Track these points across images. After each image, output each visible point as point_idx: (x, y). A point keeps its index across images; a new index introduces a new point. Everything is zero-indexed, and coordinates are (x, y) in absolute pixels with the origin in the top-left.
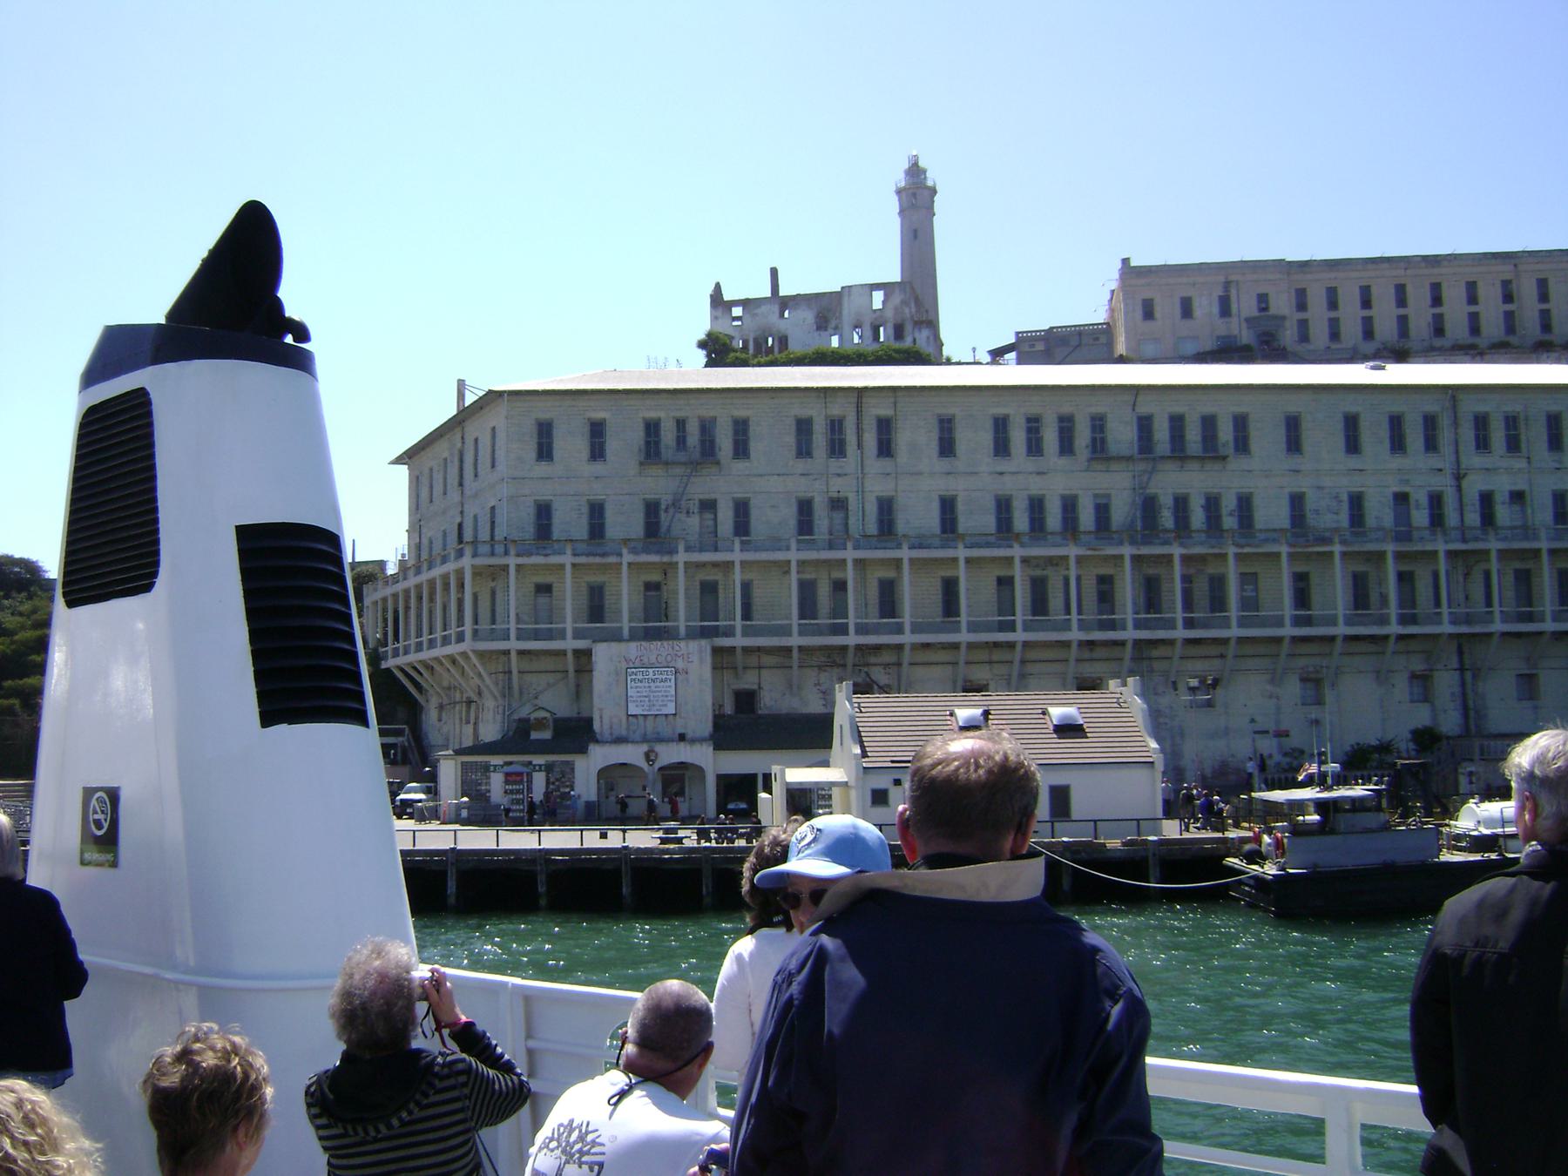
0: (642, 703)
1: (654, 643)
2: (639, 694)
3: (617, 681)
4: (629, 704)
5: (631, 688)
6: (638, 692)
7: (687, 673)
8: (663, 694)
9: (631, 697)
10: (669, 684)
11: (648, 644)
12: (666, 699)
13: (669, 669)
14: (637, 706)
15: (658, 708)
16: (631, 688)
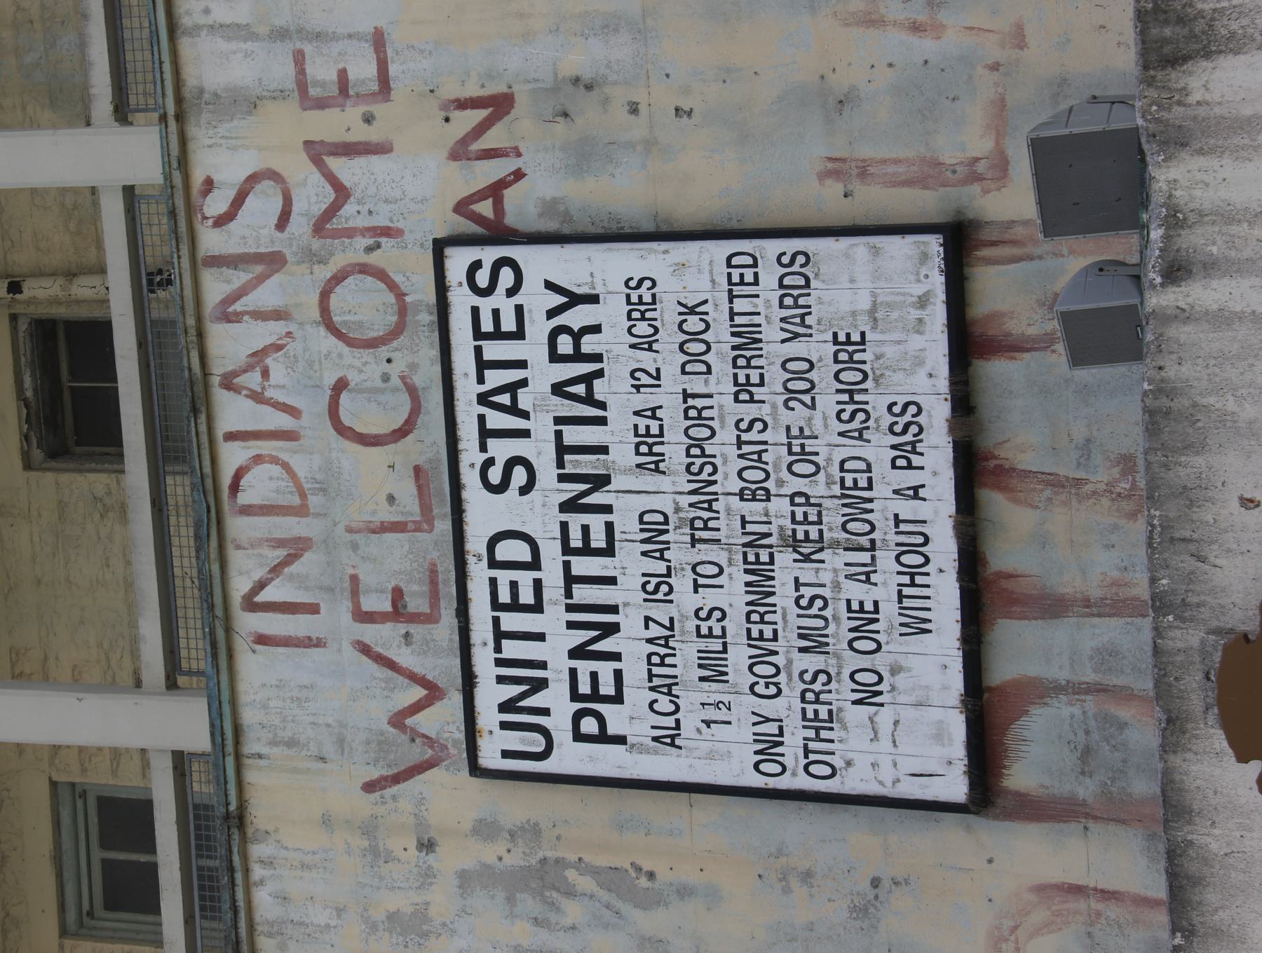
0: (839, 633)
1: (232, 456)
2: (739, 656)
3: (611, 878)
4: (849, 783)
5: (668, 739)
6: (713, 671)
7: (500, 105)
8: (721, 384)
9: (769, 748)
10: (611, 313)
11: (239, 527)
12: (774, 346)
13: (461, 301)
14: (868, 696)
15: (878, 450)
16: (668, 739)
